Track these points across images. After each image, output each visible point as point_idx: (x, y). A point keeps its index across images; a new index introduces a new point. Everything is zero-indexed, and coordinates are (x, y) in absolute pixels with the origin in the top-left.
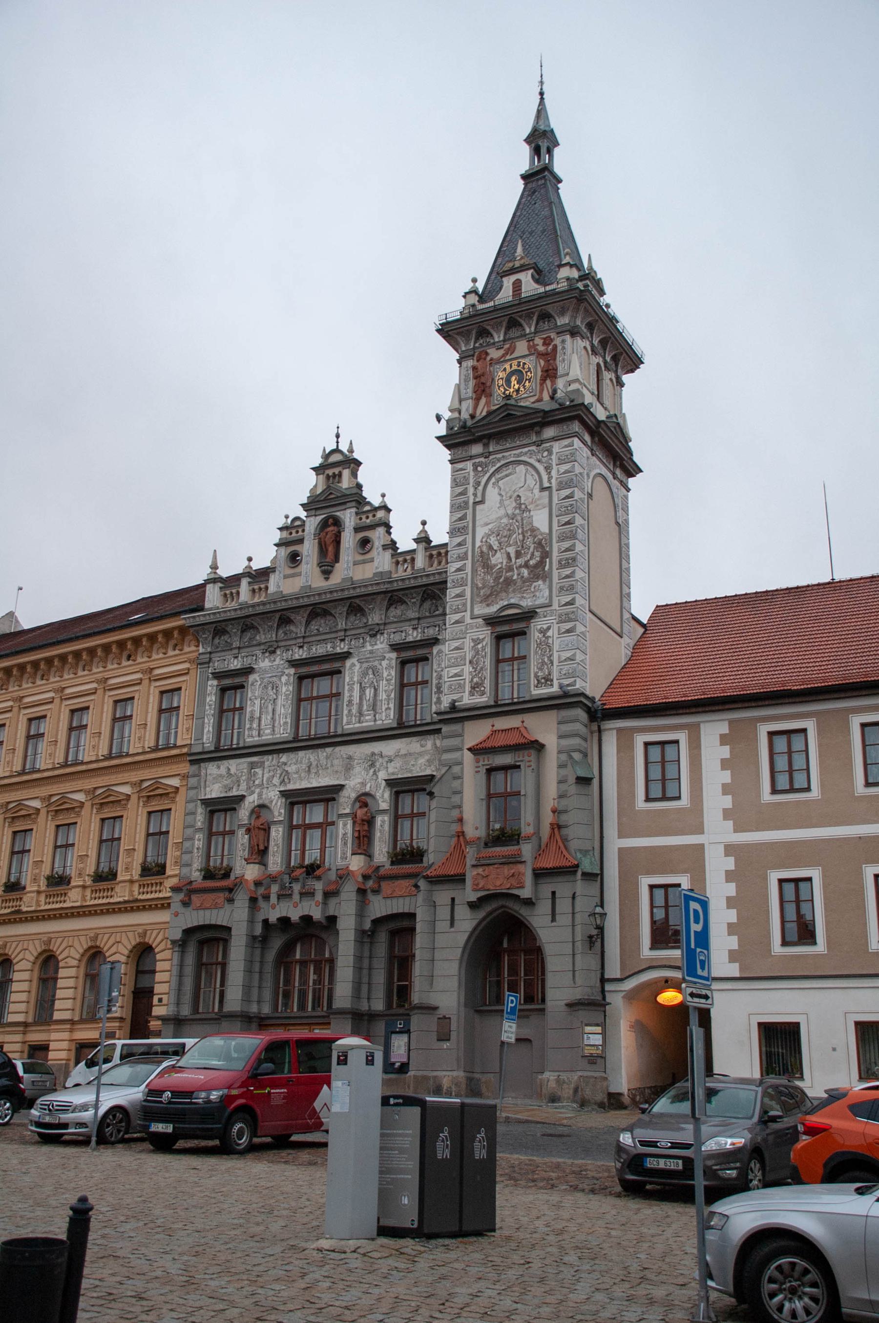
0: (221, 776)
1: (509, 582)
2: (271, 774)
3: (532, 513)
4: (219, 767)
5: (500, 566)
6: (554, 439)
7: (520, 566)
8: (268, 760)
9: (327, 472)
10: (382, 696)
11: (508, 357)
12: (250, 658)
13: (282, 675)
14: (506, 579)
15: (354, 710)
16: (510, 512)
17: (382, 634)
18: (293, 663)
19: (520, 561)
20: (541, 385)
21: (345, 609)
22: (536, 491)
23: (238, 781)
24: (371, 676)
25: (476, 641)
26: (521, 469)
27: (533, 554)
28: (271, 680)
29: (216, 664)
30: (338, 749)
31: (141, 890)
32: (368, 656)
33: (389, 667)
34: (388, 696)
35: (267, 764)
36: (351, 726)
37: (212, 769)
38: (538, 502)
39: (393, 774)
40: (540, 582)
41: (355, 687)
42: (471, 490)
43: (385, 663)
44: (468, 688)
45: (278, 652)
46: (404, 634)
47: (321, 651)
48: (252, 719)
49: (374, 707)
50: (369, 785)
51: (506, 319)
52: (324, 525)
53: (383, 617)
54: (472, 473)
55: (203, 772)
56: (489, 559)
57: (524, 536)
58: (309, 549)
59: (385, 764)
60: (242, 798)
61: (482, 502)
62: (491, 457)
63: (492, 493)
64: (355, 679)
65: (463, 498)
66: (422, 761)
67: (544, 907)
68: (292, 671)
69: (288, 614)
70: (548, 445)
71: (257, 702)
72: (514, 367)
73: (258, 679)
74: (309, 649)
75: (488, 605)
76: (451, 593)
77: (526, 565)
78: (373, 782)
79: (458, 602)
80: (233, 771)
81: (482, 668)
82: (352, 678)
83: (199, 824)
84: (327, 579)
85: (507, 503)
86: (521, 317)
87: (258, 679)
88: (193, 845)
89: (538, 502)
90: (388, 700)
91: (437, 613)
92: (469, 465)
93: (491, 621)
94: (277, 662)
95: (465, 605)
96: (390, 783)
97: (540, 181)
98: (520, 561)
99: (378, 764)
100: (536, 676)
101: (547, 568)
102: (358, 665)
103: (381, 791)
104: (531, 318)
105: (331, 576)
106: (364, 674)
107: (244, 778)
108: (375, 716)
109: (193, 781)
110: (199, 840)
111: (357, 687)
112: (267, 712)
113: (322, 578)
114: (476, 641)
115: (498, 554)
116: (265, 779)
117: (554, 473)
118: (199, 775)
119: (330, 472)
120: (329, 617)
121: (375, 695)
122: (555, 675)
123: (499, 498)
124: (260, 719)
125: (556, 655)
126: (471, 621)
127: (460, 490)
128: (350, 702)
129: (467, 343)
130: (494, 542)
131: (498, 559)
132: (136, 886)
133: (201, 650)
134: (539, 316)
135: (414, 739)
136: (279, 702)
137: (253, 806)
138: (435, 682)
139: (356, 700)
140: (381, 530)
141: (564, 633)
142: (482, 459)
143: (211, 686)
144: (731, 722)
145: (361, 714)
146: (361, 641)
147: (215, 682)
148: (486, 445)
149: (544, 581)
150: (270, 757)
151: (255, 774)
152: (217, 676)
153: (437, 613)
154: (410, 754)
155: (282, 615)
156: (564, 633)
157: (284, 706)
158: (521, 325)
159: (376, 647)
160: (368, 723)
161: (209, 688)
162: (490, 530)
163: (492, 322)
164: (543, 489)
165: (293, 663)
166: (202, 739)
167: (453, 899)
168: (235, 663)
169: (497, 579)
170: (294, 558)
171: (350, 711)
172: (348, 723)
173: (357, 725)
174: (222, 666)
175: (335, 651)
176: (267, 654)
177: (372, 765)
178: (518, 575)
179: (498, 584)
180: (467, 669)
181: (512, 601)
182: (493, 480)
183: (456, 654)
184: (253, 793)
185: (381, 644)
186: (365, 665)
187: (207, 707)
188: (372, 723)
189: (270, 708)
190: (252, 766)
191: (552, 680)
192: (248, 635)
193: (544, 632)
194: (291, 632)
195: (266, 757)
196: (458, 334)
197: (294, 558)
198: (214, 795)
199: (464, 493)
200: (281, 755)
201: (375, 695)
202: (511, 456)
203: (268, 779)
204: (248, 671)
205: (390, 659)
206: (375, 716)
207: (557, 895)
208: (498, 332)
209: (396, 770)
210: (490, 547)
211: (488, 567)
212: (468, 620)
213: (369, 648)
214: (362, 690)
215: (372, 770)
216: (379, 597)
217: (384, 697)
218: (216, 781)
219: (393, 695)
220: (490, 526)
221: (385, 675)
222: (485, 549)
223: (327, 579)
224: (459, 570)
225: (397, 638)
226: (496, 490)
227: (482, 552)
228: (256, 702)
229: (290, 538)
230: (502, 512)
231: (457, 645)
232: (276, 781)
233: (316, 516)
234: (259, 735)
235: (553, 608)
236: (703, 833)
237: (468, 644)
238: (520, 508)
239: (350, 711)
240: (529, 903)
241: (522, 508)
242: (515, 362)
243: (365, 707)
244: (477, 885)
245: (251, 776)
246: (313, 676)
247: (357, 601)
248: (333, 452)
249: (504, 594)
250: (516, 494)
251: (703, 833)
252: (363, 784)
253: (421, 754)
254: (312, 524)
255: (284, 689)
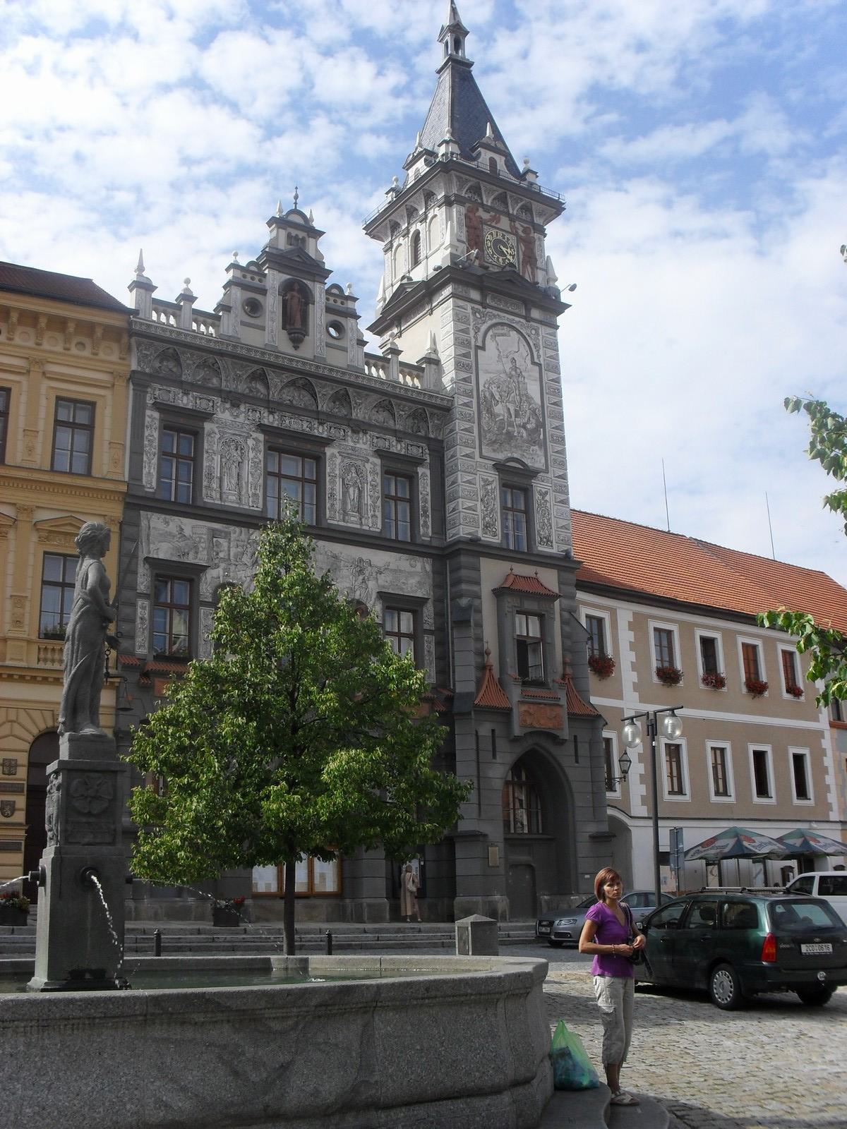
0: (170, 534)
1: (510, 436)
2: (240, 549)
3: (526, 381)
4: (167, 523)
5: (501, 417)
6: (541, 322)
7: (519, 426)
8: (235, 532)
9: (290, 230)
10: (368, 500)
11: (493, 224)
12: (204, 402)
13: (247, 437)
14: (508, 432)
15: (338, 506)
16: (508, 370)
17: (365, 433)
18: (262, 428)
19: (519, 421)
20: (523, 267)
21: (331, 393)
22: (529, 361)
23: (196, 547)
24: (354, 475)
25: (487, 483)
26: (514, 333)
27: (529, 419)
28: (234, 437)
29: (157, 393)
30: (321, 543)
31: (42, 655)
32: (350, 452)
33: (373, 472)
34: (374, 503)
35: (233, 536)
36: (336, 523)
37: (155, 523)
38: (530, 373)
39: (384, 587)
40: (536, 448)
41: (337, 480)
42: (472, 333)
43: (368, 466)
44: (481, 526)
45: (242, 408)
46: (387, 443)
47: (295, 426)
48: (210, 475)
49: (359, 511)
50: (358, 593)
51: (501, 191)
52: (287, 288)
53: (367, 417)
54: (471, 317)
55: (144, 523)
56: (491, 406)
57: (521, 399)
58: (272, 303)
59: (374, 574)
60: (202, 569)
61: (483, 348)
62: (488, 310)
63: (490, 344)
64: (337, 472)
65: (464, 336)
66: (413, 581)
67: (570, 748)
68: (261, 437)
69: (268, 371)
70: (535, 324)
71: (217, 458)
72: (500, 237)
73: (216, 431)
74: (282, 420)
75: (494, 451)
76: (459, 425)
77: (524, 427)
78: (363, 590)
79: (466, 436)
80: (187, 532)
81: (492, 510)
82: (333, 470)
83: (142, 587)
84: (296, 348)
85: (504, 360)
86: (511, 197)
87: (216, 431)
88: (135, 611)
89: (530, 373)
90: (374, 507)
91: (420, 434)
92: (469, 306)
93: (499, 467)
94: (241, 419)
95: (473, 441)
96: (382, 596)
97: (460, 71)
98: (519, 421)
99: (367, 573)
100: (539, 534)
101: (542, 437)
102: (338, 460)
103: (372, 602)
104: (517, 203)
105: (302, 346)
106: (347, 470)
107: (203, 545)
108: (361, 519)
109: (129, 530)
110: (144, 608)
111: (339, 482)
112: (230, 476)
113: (291, 344)
114: (487, 483)
115: (500, 405)
116: (232, 554)
117: (541, 352)
118: (137, 525)
119: (294, 232)
120: (303, 392)
121: (360, 496)
122: (554, 538)
123: (497, 353)
124: (221, 480)
125: (553, 521)
126: (479, 460)
127: (463, 327)
128: (332, 495)
129: (460, 189)
130: (494, 390)
131: (499, 409)
132: (35, 648)
133: (134, 367)
134: (522, 205)
135: (404, 556)
136: (247, 467)
137: (216, 582)
138: (421, 504)
139: (339, 495)
140: (352, 321)
141: (559, 502)
142: (480, 307)
143: (151, 417)
144: (634, 614)
145: (345, 513)
146: (342, 433)
147: (156, 415)
148: (484, 296)
149: (540, 447)
150: (237, 529)
151: (218, 544)
152: (157, 406)
153: (420, 434)
154: (401, 571)
155: (260, 368)
156: (559, 502)
157: (252, 474)
158: (506, 204)
159: (358, 445)
160: (353, 523)
161: (147, 419)
162: (491, 378)
163: (489, 186)
164: (533, 363)
165: (262, 428)
166: (141, 480)
167: (493, 731)
168: (185, 401)
169: (501, 428)
170: (254, 308)
171: (332, 505)
172: (333, 518)
173: (342, 523)
174: (166, 398)
175: (312, 433)
176: (228, 405)
177: (361, 572)
178: (519, 433)
179: (501, 434)
180: (480, 506)
181: (515, 455)
182: (490, 333)
183: (468, 487)
184: (217, 566)
185: (364, 444)
186: (347, 461)
187: (146, 442)
188: (358, 527)
189: (234, 471)
190: (214, 534)
191: (552, 543)
192: (202, 374)
193: (544, 494)
194: (258, 391)
195: (232, 528)
196: (456, 176)
197: (254, 308)
198: (161, 556)
199: (466, 331)
200: (251, 531)
201: (360, 496)
202: (507, 318)
203: (236, 556)
204: (207, 416)
205: (375, 465)
206: (361, 519)
207: (579, 739)
208: (488, 197)
209: (385, 582)
210: (492, 396)
211: (490, 411)
212: (477, 458)
213: (352, 444)
214: (345, 486)
215: (361, 577)
216: (375, 396)
217: (370, 502)
218: (165, 537)
219: (379, 503)
220: (492, 375)
221: (370, 479)
222: (487, 394)
223: (296, 348)
224: (465, 405)
225: (381, 444)
226: (494, 344)
227: (485, 397)
228: (215, 458)
229: (246, 282)
230: (500, 367)
231: (469, 478)
232: (246, 559)
233: (280, 272)
234: (221, 498)
235: (549, 475)
236: (622, 699)
237: (479, 483)
238: (516, 371)
239: (332, 505)
240: (563, 742)
241: (516, 373)
242: (500, 233)
243: (349, 507)
244: (525, 721)
245: (213, 547)
246: (281, 451)
247: (350, 391)
248: (291, 212)
249: (507, 446)
250: (511, 356)
251: (622, 699)
252: (352, 590)
253: (411, 574)
254: (274, 279)
255: (251, 455)
